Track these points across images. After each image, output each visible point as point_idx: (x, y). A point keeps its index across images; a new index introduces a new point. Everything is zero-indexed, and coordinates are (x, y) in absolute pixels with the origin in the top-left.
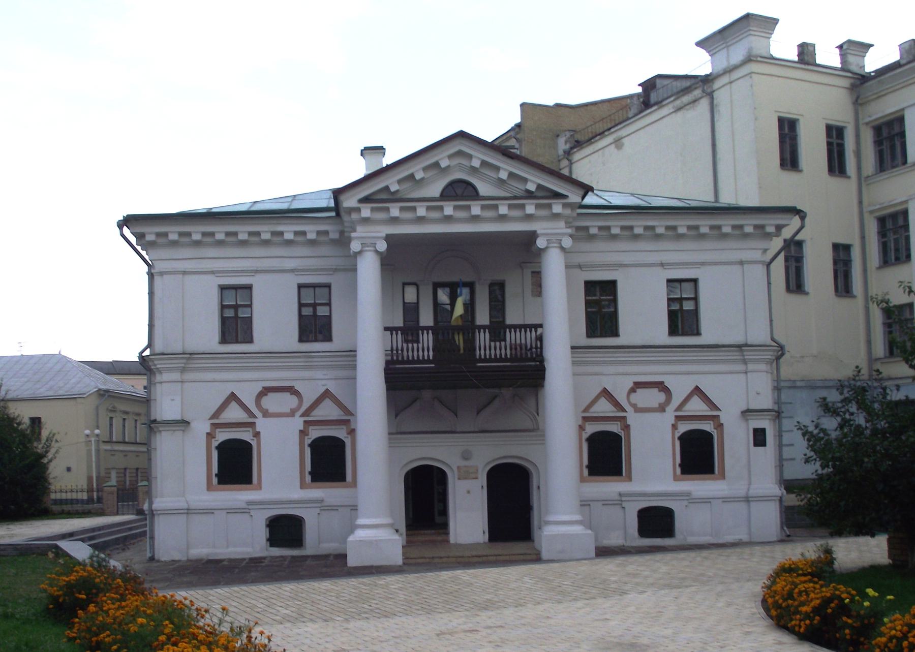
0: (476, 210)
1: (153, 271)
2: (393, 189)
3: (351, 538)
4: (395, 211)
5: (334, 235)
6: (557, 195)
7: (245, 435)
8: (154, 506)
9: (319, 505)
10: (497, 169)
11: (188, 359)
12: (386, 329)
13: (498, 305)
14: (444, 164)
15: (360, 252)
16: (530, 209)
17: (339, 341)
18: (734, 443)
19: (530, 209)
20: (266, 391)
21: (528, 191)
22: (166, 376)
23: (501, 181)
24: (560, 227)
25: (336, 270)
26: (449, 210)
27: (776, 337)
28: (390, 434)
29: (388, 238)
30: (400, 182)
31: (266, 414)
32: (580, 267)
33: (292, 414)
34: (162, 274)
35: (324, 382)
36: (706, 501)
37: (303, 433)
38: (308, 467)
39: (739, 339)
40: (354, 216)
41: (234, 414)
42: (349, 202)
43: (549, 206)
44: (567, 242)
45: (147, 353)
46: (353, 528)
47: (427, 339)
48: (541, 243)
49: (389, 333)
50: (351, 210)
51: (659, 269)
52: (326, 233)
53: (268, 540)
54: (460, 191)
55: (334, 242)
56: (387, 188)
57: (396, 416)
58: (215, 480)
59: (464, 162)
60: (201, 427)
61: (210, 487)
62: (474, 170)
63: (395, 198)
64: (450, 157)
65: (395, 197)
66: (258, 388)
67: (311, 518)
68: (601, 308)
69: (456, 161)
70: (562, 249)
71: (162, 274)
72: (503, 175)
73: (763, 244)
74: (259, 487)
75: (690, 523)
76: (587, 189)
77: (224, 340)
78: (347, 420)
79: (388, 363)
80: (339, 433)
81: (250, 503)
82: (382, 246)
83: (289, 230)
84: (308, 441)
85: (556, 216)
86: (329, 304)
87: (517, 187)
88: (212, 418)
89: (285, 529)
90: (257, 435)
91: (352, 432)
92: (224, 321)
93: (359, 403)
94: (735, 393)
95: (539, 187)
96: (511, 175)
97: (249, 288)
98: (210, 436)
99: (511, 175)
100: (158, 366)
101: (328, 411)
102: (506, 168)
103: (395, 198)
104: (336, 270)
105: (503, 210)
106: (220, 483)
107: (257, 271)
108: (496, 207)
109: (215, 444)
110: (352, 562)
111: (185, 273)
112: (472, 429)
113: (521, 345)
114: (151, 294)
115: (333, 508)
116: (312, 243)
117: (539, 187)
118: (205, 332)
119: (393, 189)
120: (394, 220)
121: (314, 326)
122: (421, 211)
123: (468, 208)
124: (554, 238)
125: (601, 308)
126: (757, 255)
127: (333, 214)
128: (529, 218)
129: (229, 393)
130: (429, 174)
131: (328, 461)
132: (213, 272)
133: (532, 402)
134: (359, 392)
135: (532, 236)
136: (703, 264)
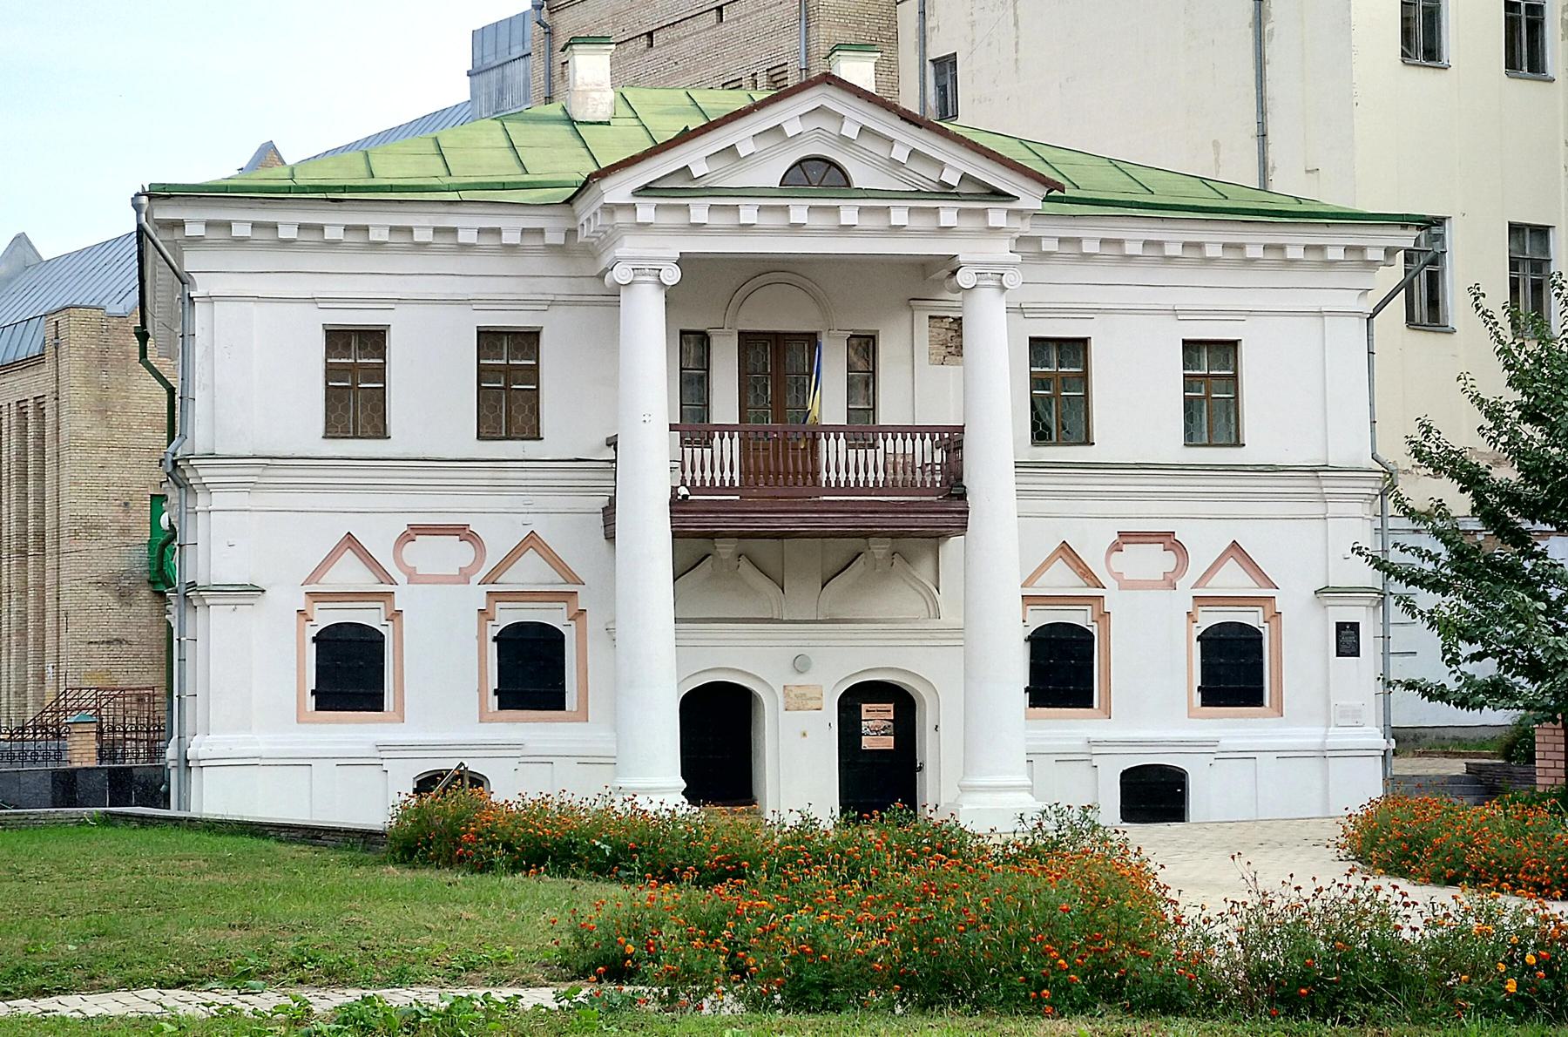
5: (555, 238)
6: (997, 194)
13: (863, 380)
18: (1297, 655)
21: (942, 183)
22: (219, 500)
25: (553, 303)
26: (799, 212)
27: (1383, 458)
29: (684, 261)
31: (413, 577)
33: (464, 577)
36: (1247, 755)
39: (1311, 457)
40: (621, 218)
41: (350, 574)
48: (964, 278)
51: (1169, 321)
52: (541, 232)
55: (551, 248)
56: (686, 169)
59: (830, 126)
60: (286, 597)
65: (701, 184)
69: (812, 123)
71: (210, 299)
72: (900, 154)
73: (1362, 280)
77: (331, 432)
81: (381, 747)
82: (672, 276)
87: (927, 176)
92: (330, 393)
101: (530, 573)
104: (553, 303)
105: (899, 216)
122: (748, 214)
126: (1350, 302)
133: (924, 570)
135: (951, 266)
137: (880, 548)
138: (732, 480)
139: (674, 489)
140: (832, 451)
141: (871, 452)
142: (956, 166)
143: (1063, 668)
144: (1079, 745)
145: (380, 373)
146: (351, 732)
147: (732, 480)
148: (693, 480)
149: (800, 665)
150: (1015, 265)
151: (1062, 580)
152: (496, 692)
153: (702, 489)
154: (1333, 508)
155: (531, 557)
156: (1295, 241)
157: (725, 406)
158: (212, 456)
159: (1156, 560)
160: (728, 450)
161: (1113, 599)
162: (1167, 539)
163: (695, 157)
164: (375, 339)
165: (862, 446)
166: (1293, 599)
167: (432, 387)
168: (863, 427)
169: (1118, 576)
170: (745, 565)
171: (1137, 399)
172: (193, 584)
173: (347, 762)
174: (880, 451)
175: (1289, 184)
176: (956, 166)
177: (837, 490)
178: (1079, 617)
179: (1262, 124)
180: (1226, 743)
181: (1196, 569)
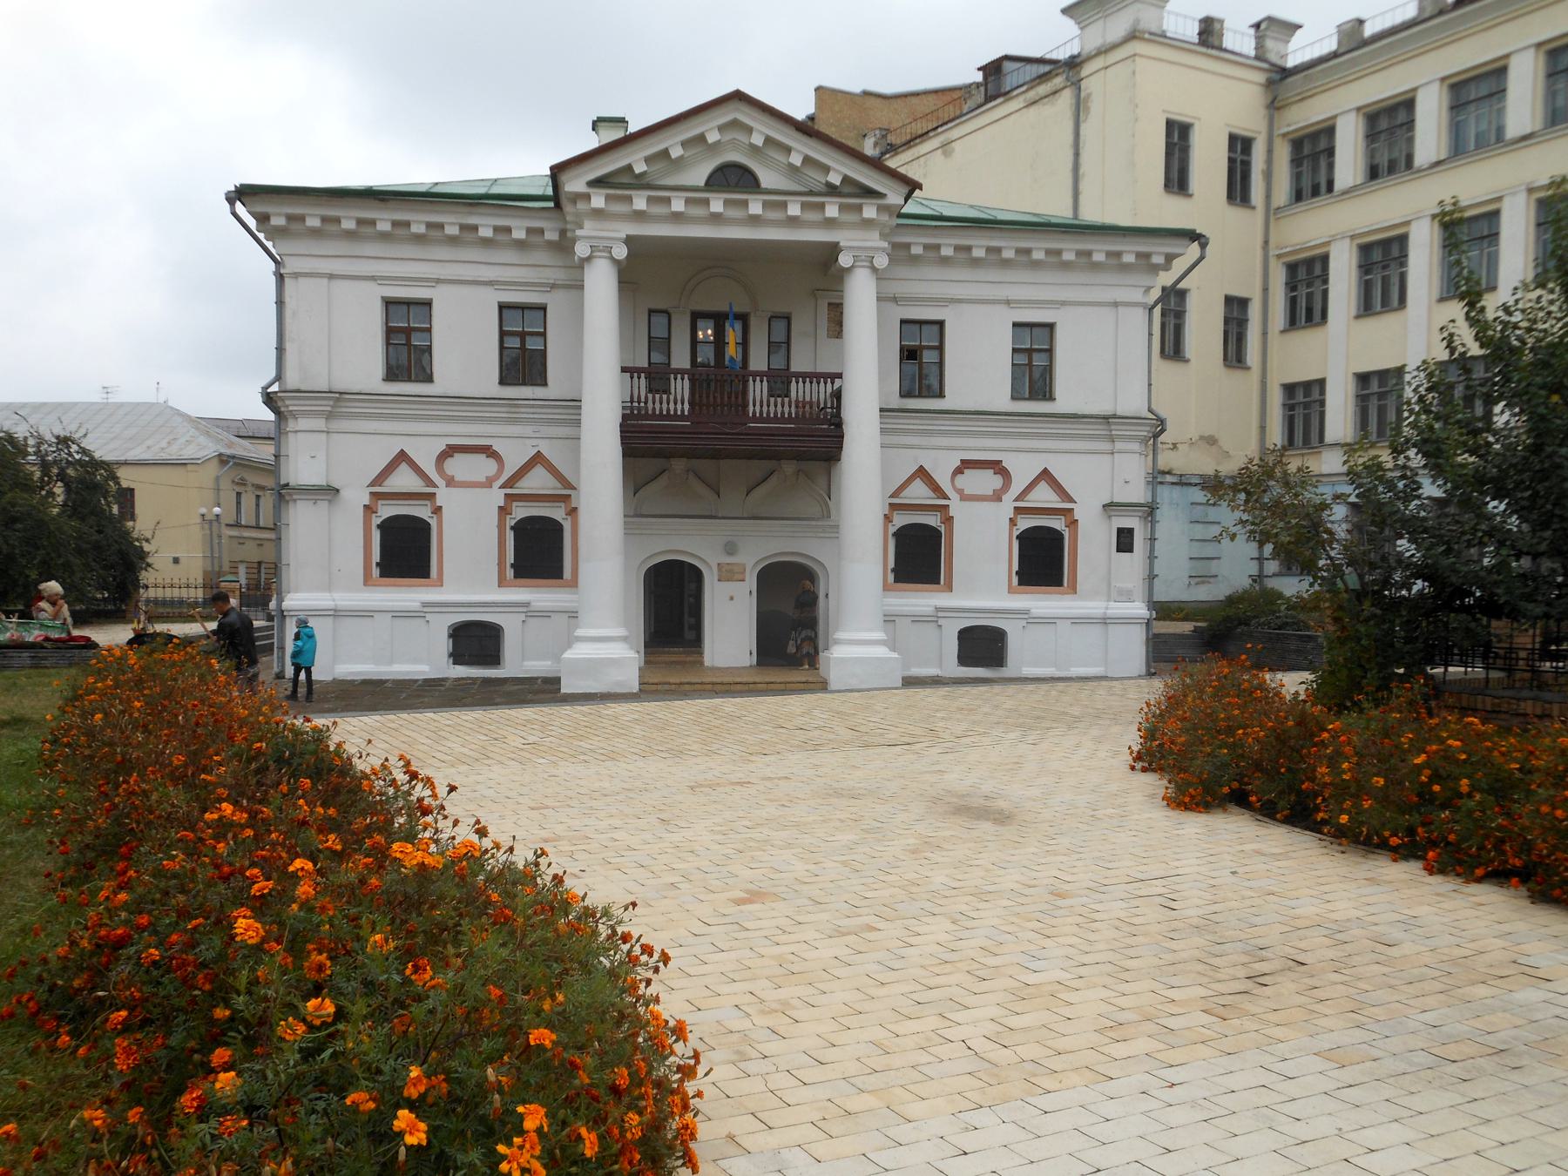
0: (755, 208)
2: (637, 171)
3: (568, 655)
4: (640, 203)
5: (551, 235)
6: (870, 193)
7: (422, 511)
8: (286, 604)
10: (788, 150)
11: (338, 400)
13: (781, 346)
14: (712, 137)
15: (589, 259)
17: (557, 385)
18: (1091, 546)
19: (832, 211)
20: (451, 451)
21: (829, 185)
22: (303, 423)
23: (791, 166)
24: (873, 240)
25: (553, 286)
26: (717, 206)
29: (629, 241)
30: (648, 160)
31: (451, 482)
32: (895, 300)
33: (488, 483)
34: (296, 275)
35: (535, 442)
37: (503, 511)
39: (1104, 408)
40: (581, 206)
41: (403, 480)
42: (575, 184)
43: (859, 208)
44: (882, 261)
45: (275, 388)
46: (571, 641)
47: (681, 388)
48: (844, 260)
51: (1002, 309)
52: (541, 231)
53: (451, 655)
55: (551, 245)
56: (629, 168)
59: (742, 137)
60: (356, 496)
61: (367, 580)
62: (753, 147)
63: (640, 182)
64: (721, 128)
66: (440, 446)
67: (510, 625)
68: (920, 360)
69: (728, 136)
70: (874, 269)
71: (296, 275)
72: (796, 159)
75: (1022, 653)
76: (913, 186)
77: (392, 374)
78: (565, 495)
79: (624, 417)
80: (557, 513)
81: (425, 604)
82: (621, 252)
83: (486, 225)
84: (510, 522)
85: (868, 224)
86: (544, 335)
87: (816, 178)
88: (372, 484)
90: (437, 510)
91: (573, 512)
93: (584, 471)
94: (1097, 481)
96: (807, 160)
97: (428, 304)
99: (807, 160)
101: (538, 481)
102: (802, 148)
103: (640, 182)
104: (553, 286)
105: (794, 210)
106: (382, 575)
107: (438, 281)
108: (784, 205)
109: (376, 521)
110: (565, 689)
111: (331, 277)
114: (280, 303)
115: (545, 614)
116: (520, 245)
118: (361, 361)
119: (637, 171)
120: (640, 216)
121: (523, 362)
122: (678, 205)
123: (745, 204)
124: (863, 254)
125: (920, 360)
126: (1137, 296)
127: (551, 204)
128: (830, 223)
131: (538, 550)
132: (373, 278)
134: (583, 456)
135: (834, 249)
136: (1064, 303)
137: (789, 467)
142: (840, 169)
143: (919, 555)
144: (930, 610)
146: (406, 595)
149: (730, 549)
150: (883, 250)
151: (918, 492)
152: (512, 566)
154: (1119, 445)
156: (1100, 250)
159: (986, 481)
161: (956, 508)
162: (997, 467)
166: (1087, 512)
167: (465, 351)
168: (780, 380)
169: (960, 492)
171: (978, 368)
173: (400, 615)
175: (1091, 213)
178: (932, 520)
179: (1077, 154)
180: (1035, 612)
181: (1017, 487)
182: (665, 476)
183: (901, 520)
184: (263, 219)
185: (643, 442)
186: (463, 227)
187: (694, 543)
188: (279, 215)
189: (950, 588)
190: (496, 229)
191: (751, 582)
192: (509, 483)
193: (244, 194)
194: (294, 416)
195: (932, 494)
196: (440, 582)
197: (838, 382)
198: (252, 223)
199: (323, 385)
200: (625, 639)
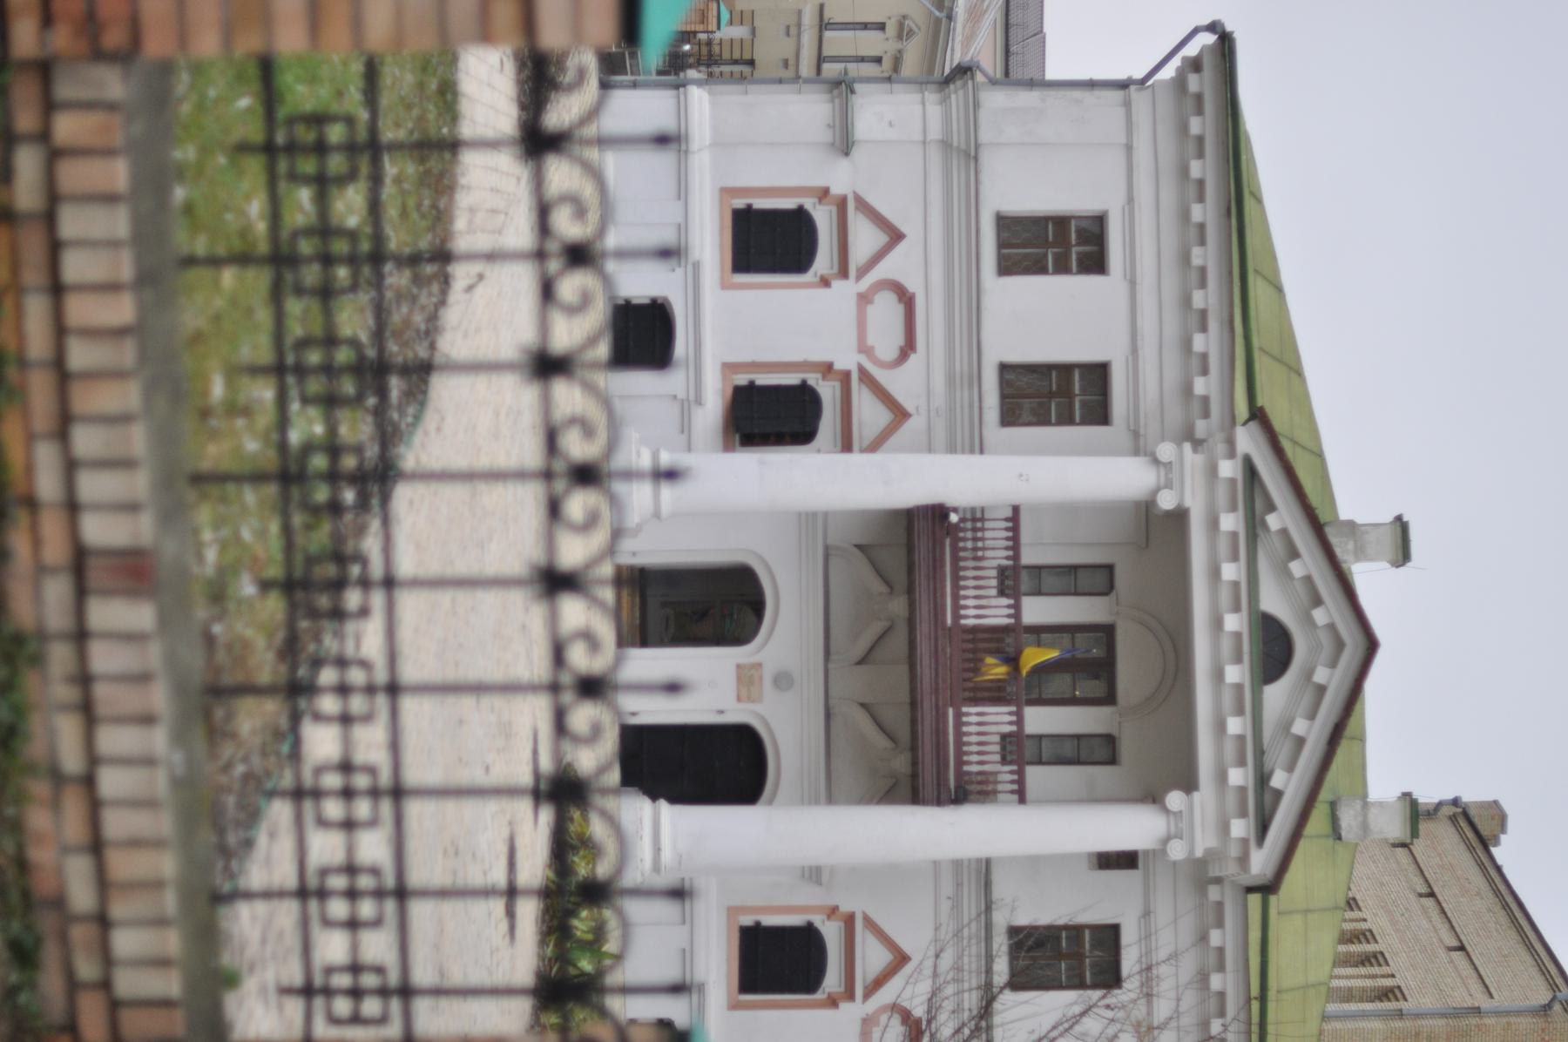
1: (1132, 88)
5: (1201, 427)
6: (1263, 827)
7: (824, 260)
9: (692, 397)
11: (967, 155)
12: (1016, 509)
15: (1156, 461)
16: (1236, 777)
20: (907, 300)
21: (1271, 773)
22: (935, 112)
26: (1233, 622)
28: (826, 514)
29: (1179, 517)
30: (1284, 532)
31: (864, 299)
33: (864, 348)
34: (1127, 104)
37: (827, 369)
38: (763, 380)
40: (1221, 448)
41: (864, 239)
43: (1243, 814)
44: (1177, 851)
48: (1175, 799)
49: (1009, 513)
50: (1231, 443)
52: (1206, 414)
54: (1273, 649)
56: (1271, 507)
57: (858, 547)
58: (740, 203)
60: (841, 177)
61: (727, 192)
62: (1309, 673)
63: (1254, 526)
66: (913, 285)
67: (670, 382)
69: (1325, 638)
70: (1166, 840)
71: (1127, 104)
72: (1299, 727)
74: (725, 286)
77: (1005, 223)
81: (697, 266)
82: (1166, 502)
85: (1225, 828)
87: (1277, 756)
89: (644, 335)
90: (825, 282)
95: (1278, 794)
96: (1300, 742)
98: (823, 194)
100: (953, 96)
102: (1313, 731)
107: (1133, 283)
111: (1129, 148)
112: (832, 693)
113: (996, 782)
114: (1091, 85)
116: (1187, 390)
117: (1278, 794)
118: (1027, 186)
123: (1238, 660)
124: (1184, 825)
128: (1222, 777)
129: (904, 228)
130: (1300, 589)
131: (771, 414)
132: (1130, 200)
135: (1189, 784)
138: (966, 617)
139: (955, 510)
140: (999, 718)
141: (997, 758)
142: (1289, 783)
145: (1062, 268)
147: (966, 617)
148: (964, 530)
149: (783, 681)
150: (1192, 850)
151: (872, 957)
153: (956, 540)
155: (883, 417)
157: (1037, 610)
158: (976, 105)
160: (997, 613)
163: (1283, 518)
164: (1095, 264)
165: (1003, 748)
167: (1046, 318)
170: (878, 627)
172: (853, 92)
174: (999, 767)
176: (1289, 783)
177: (959, 724)
178: (832, 979)
182: (884, 589)
183: (831, 933)
184: (1195, 64)
185: (920, 542)
186: (1203, 314)
187: (789, 632)
188: (1201, 84)
189: (734, 1006)
190: (1204, 357)
191: (735, 714)
192: (865, 376)
193: (1226, 43)
194: (944, 101)
195: (871, 976)
196: (725, 286)
197: (1016, 797)
198: (1192, 50)
199: (985, 136)
200: (657, 514)
